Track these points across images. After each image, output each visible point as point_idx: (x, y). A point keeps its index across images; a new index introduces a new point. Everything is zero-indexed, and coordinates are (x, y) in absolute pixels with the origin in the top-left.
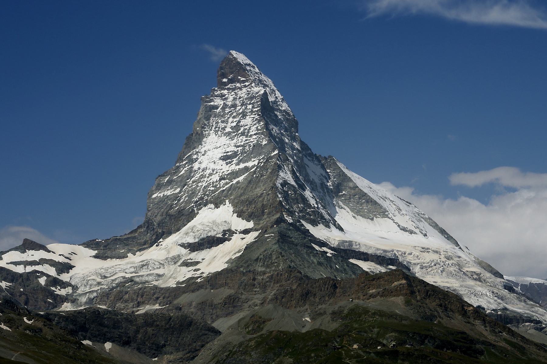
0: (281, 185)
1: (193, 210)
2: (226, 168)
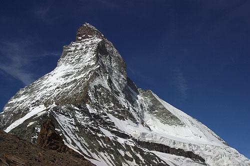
0: (95, 86)
1: (28, 109)
2: (63, 81)
